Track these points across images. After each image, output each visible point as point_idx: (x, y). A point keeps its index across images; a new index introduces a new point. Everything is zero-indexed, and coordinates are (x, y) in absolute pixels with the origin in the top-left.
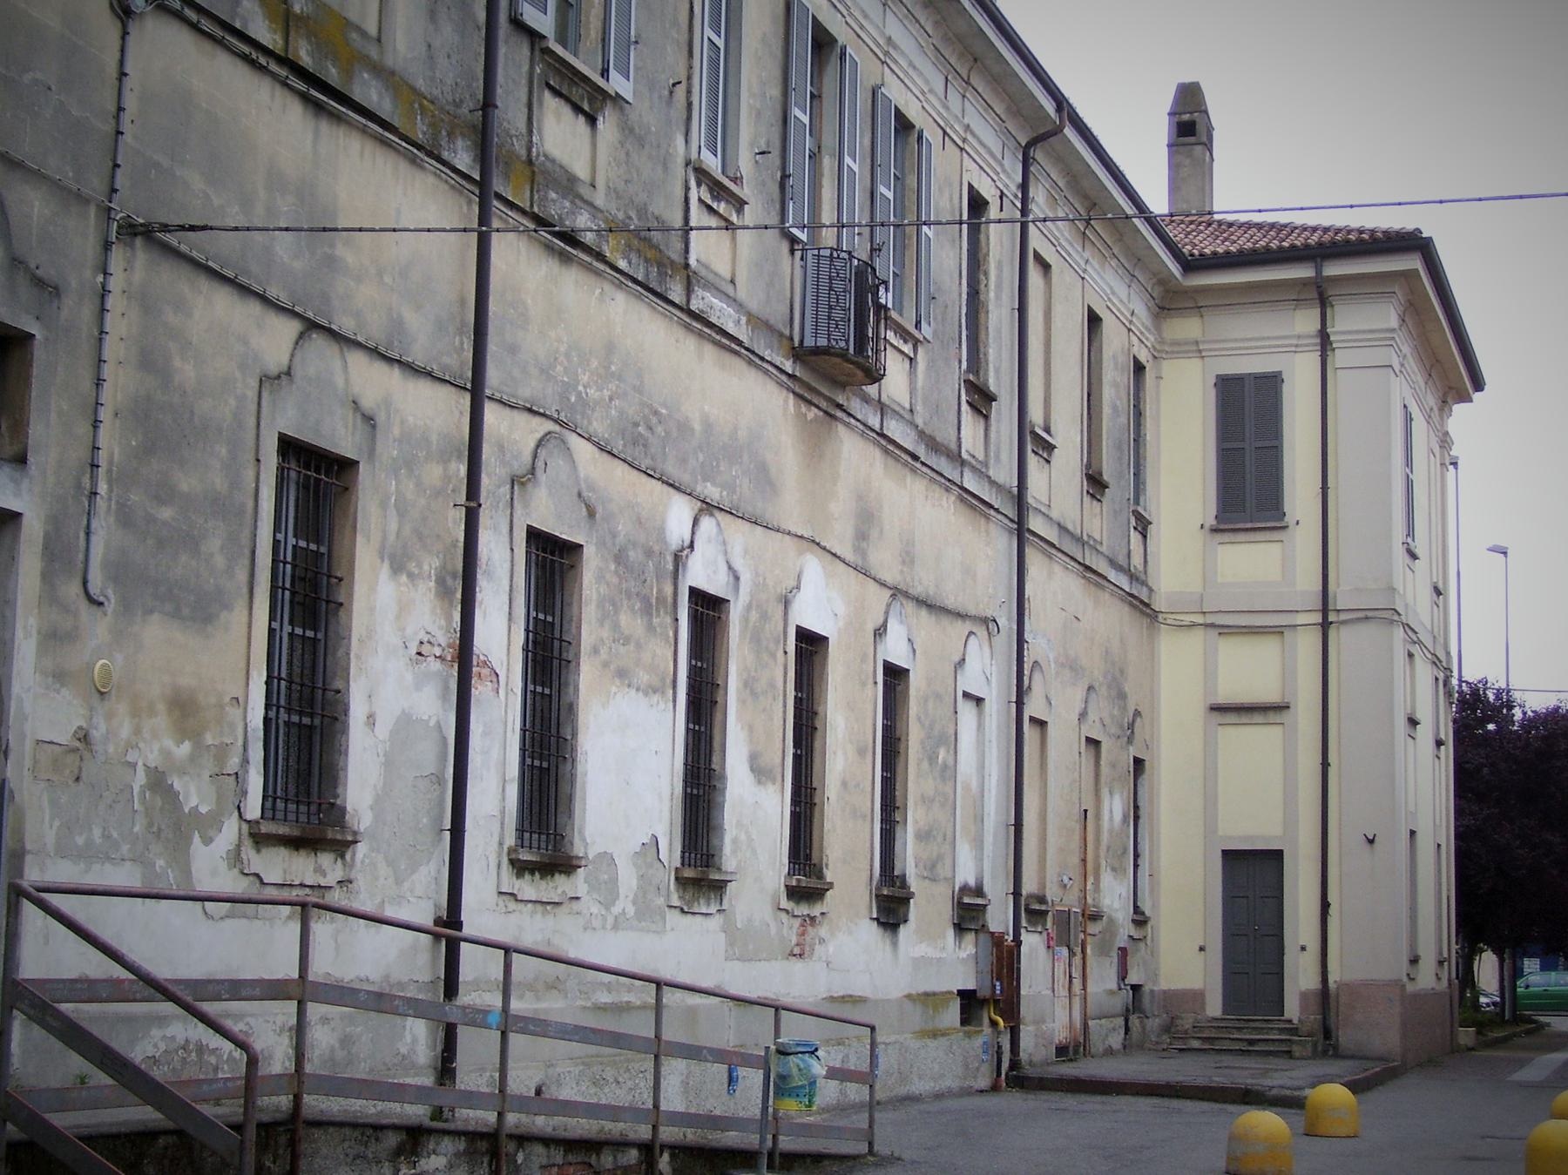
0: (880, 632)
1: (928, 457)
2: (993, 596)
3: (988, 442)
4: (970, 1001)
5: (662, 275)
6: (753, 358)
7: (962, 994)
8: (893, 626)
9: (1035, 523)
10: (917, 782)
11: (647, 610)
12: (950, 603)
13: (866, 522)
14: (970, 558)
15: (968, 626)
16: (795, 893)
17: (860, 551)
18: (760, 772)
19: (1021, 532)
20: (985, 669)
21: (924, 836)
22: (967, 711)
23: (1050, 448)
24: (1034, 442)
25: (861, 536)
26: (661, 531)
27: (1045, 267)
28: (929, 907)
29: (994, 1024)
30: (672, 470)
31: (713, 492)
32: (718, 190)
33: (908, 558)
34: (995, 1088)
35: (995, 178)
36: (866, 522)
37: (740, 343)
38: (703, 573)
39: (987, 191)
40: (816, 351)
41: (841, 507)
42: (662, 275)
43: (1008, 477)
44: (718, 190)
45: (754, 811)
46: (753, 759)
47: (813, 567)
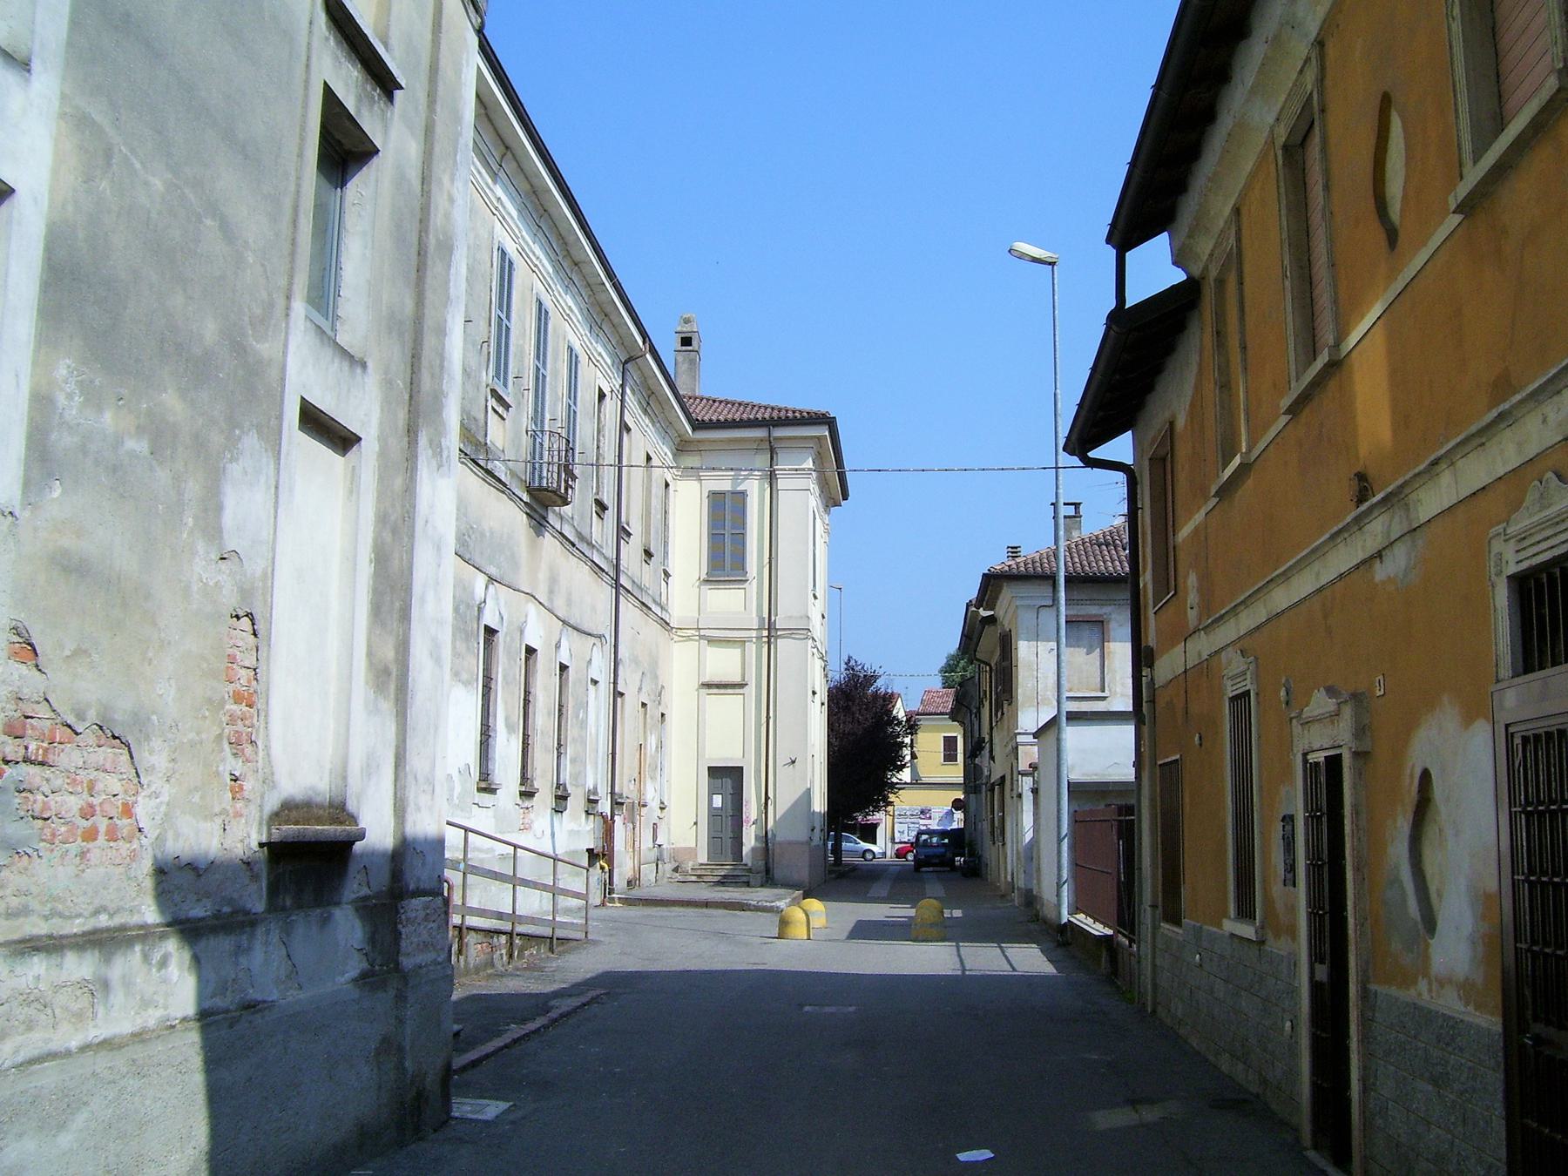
0: (558, 646)
1: (576, 545)
2: (604, 626)
3: (601, 532)
4: (593, 855)
5: (477, 451)
6: (512, 496)
7: (590, 851)
8: (564, 643)
9: (623, 580)
10: (571, 732)
11: (467, 639)
12: (585, 627)
13: (553, 581)
14: (592, 598)
15: (593, 640)
16: (522, 794)
17: (551, 600)
18: (510, 728)
19: (617, 586)
20: (600, 667)
21: (573, 761)
22: (591, 687)
23: (629, 535)
24: (623, 532)
25: (551, 592)
26: (473, 593)
27: (629, 430)
28: (576, 803)
29: (602, 868)
30: (478, 560)
31: (492, 570)
32: (500, 399)
33: (569, 603)
34: (603, 904)
35: (610, 383)
36: (553, 581)
37: (505, 485)
38: (490, 619)
39: (606, 390)
40: (541, 489)
41: (543, 575)
42: (477, 451)
43: (611, 554)
44: (500, 399)
45: (507, 748)
46: (507, 719)
47: (532, 609)
